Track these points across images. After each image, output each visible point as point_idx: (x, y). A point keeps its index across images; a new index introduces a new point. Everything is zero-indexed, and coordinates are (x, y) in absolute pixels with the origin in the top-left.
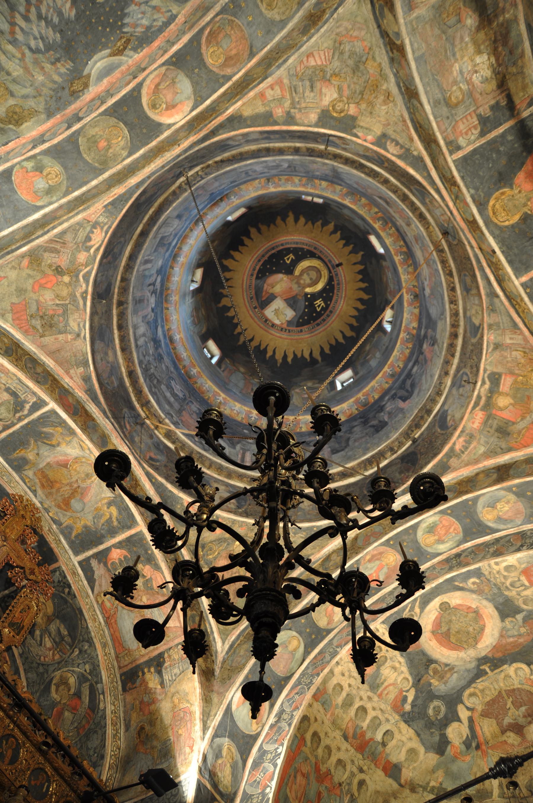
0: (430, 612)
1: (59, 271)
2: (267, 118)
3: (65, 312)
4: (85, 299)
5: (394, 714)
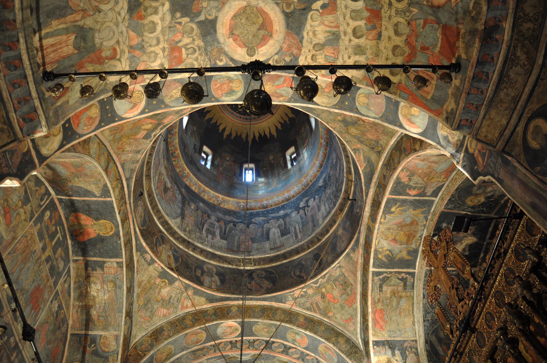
0: (263, 55)
1: (323, 296)
2: (196, 292)
3: (336, 280)
4: (324, 276)
5: (339, 5)
